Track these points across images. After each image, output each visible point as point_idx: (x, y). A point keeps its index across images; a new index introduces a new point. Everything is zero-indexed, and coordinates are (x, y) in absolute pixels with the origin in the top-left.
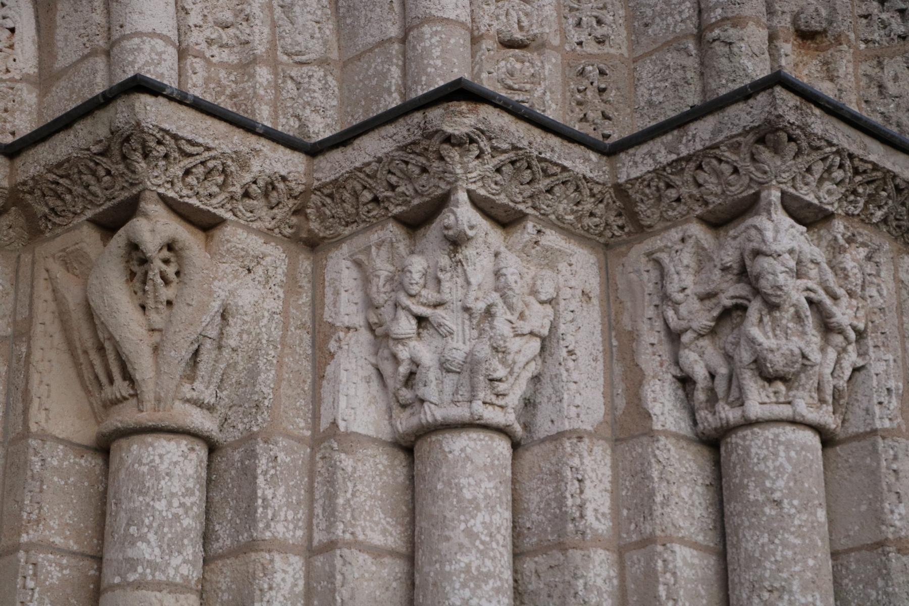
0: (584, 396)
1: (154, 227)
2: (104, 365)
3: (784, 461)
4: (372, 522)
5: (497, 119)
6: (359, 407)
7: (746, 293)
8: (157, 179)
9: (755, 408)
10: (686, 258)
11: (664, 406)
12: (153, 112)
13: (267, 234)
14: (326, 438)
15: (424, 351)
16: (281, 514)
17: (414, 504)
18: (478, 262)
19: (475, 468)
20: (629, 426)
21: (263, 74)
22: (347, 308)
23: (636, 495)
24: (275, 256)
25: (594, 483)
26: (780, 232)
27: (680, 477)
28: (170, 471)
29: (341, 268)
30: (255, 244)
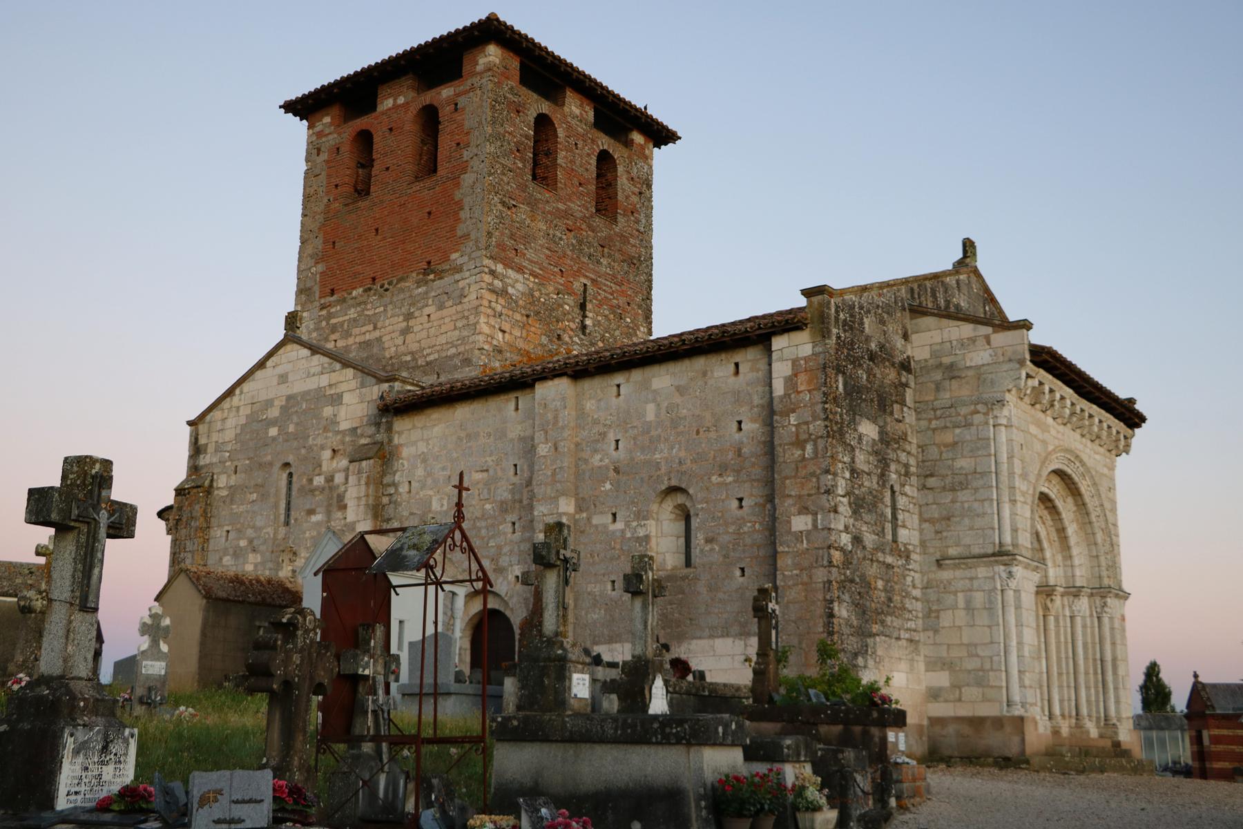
0: (1088, 613)
2: (1046, 608)
3: (1106, 620)
4: (1069, 625)
6: (1068, 614)
7: (1105, 604)
10: (1098, 600)
14: (1064, 616)
16: (1061, 623)
19: (1079, 621)
20: (1091, 615)
22: (1066, 603)
23: (1092, 623)
25: (1088, 620)
27: (1096, 620)
28: (1051, 619)
29: (1065, 599)
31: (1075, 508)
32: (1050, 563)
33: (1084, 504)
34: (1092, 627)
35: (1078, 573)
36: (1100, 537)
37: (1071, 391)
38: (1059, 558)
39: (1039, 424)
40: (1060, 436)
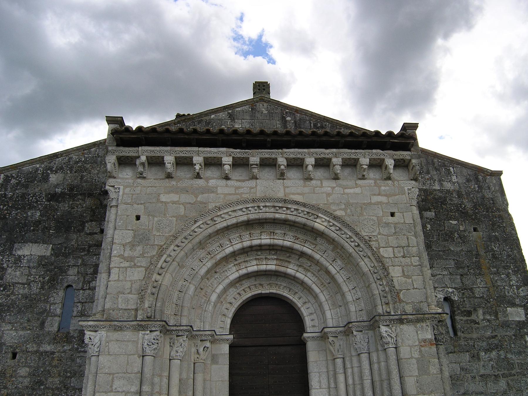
1: (331, 339)
5: (354, 324)
8: (329, 335)
9: (386, 347)
11: (380, 348)
12: (326, 330)
13: (343, 336)
14: (351, 356)
15: (356, 346)
17: (360, 361)
18: (358, 337)
21: (340, 319)
23: (378, 358)
24: (344, 338)
26: (383, 329)
28: (339, 362)
30: (342, 337)
31: (331, 247)
32: (326, 307)
33: (334, 240)
34: (379, 363)
35: (352, 308)
36: (365, 265)
37: (224, 149)
38: (339, 297)
39: (185, 191)
40: (241, 191)
